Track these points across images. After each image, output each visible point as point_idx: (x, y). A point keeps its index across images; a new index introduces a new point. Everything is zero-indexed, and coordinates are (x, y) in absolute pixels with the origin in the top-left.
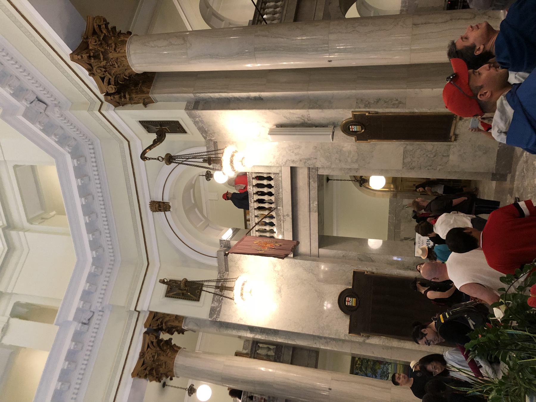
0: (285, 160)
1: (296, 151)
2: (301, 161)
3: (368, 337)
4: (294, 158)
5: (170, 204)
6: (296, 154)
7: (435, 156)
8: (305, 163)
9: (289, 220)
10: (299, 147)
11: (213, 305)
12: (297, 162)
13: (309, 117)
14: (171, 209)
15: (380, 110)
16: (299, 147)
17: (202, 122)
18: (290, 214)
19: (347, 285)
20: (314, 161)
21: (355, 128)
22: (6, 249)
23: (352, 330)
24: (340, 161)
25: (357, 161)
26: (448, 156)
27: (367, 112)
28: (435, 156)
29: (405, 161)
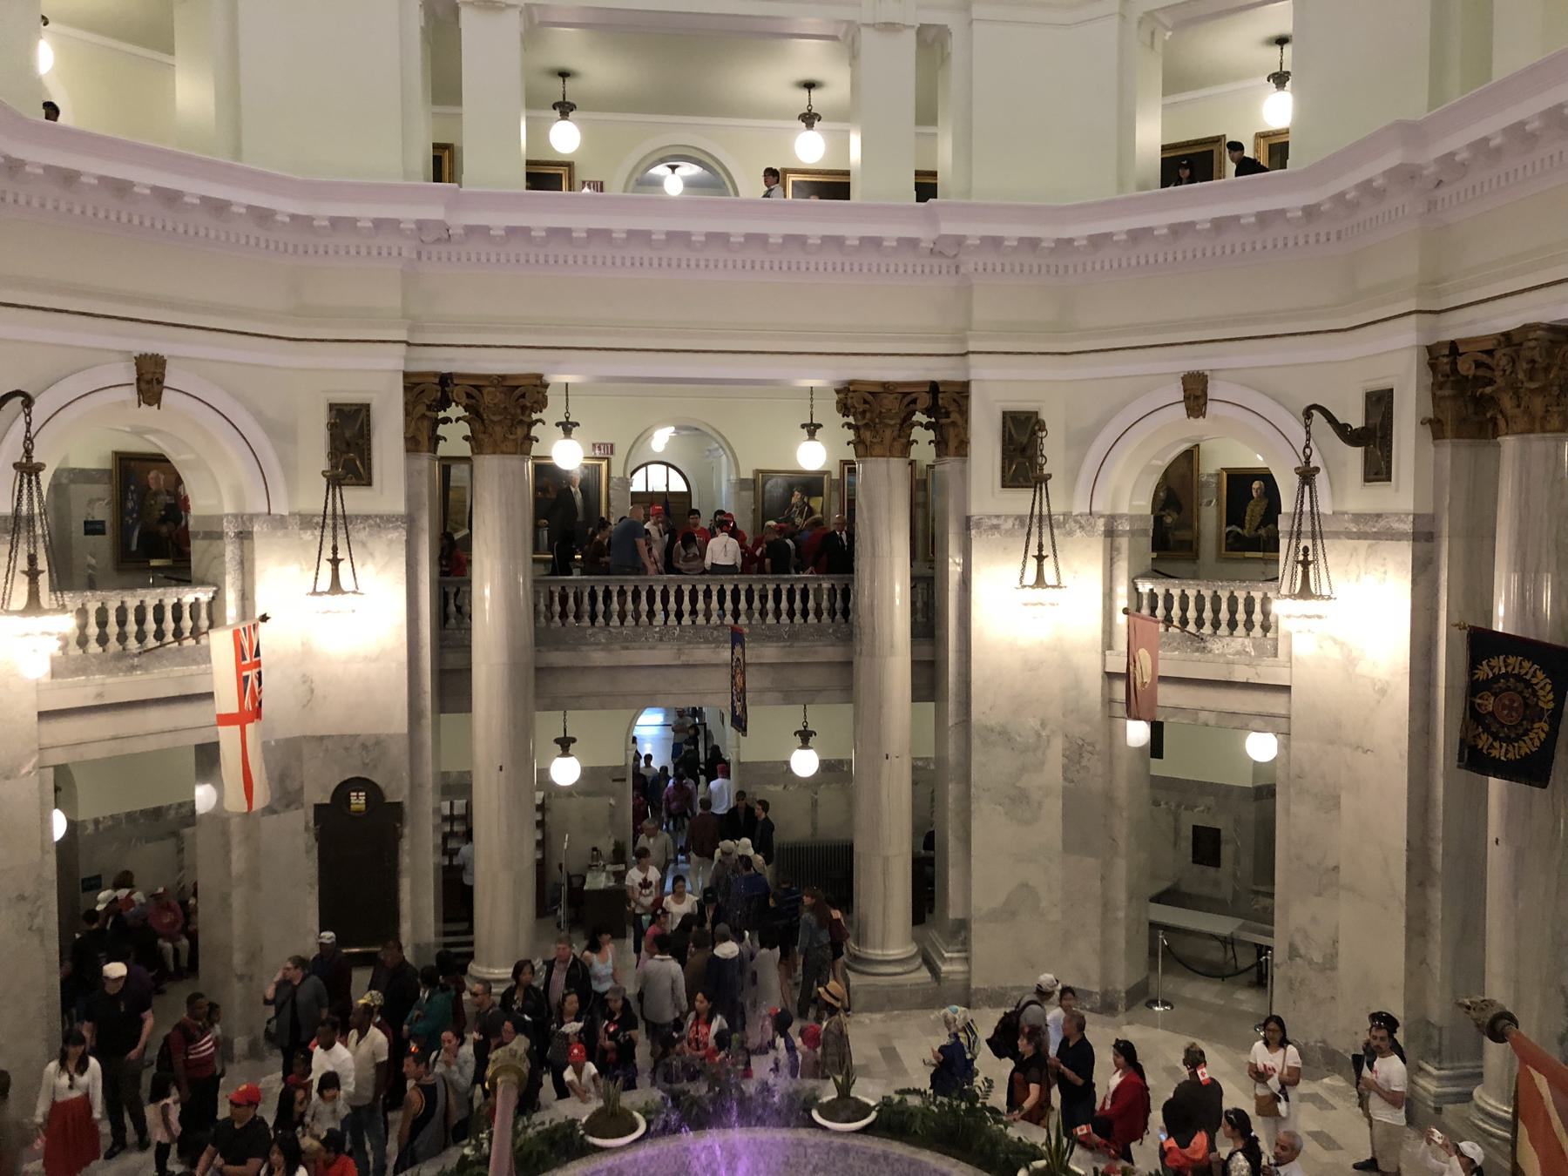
15: (405, 845)
21: (358, 801)
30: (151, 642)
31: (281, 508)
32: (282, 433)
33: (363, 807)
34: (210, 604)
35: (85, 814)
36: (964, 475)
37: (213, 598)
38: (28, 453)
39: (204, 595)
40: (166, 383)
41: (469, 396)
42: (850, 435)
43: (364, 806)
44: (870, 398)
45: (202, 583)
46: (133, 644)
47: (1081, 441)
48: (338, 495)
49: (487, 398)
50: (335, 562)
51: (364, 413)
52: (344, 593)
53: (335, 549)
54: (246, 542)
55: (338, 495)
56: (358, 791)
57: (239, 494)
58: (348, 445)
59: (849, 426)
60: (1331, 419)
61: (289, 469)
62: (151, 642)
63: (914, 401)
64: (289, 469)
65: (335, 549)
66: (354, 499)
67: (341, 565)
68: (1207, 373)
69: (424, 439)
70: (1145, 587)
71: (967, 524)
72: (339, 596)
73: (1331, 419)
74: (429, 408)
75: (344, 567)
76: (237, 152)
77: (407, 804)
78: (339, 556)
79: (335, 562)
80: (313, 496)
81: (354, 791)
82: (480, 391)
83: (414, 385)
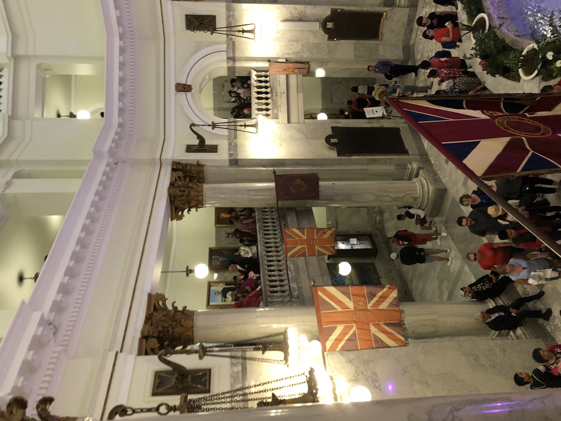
0: (283, 53)
1: (290, 48)
2: (293, 53)
3: (351, 156)
4: (289, 51)
5: (192, 86)
6: (290, 49)
7: (371, 50)
8: (296, 55)
9: (285, 96)
10: (292, 45)
11: (230, 152)
12: (290, 54)
13: (305, 13)
14: (192, 91)
15: (346, 8)
16: (292, 45)
17: (233, 15)
18: (285, 91)
19: (330, 132)
20: (302, 53)
22: (6, 135)
23: (339, 155)
24: (318, 53)
25: (328, 54)
26: (378, 50)
27: (339, 9)
28: (371, 50)
29: (356, 53)
30: (269, 90)
31: (224, 47)
32: (198, 47)
33: (332, 23)
34: (257, 71)
35: (320, 106)
37: (255, 70)
38: (209, 125)
39: (254, 73)
40: (184, 83)
42: (193, 210)
43: (332, 23)
45: (250, 73)
46: (269, 96)
48: (219, 29)
50: (243, 31)
51: (189, 17)
52: (254, 29)
53: (239, 31)
54: (236, 59)
55: (219, 29)
56: (326, 25)
58: (201, 24)
59: (189, 211)
62: (269, 90)
65: (239, 31)
66: (221, 23)
67: (245, 29)
72: (256, 31)
75: (245, 28)
76: (102, 59)
77: (331, 7)
78: (242, 30)
79: (243, 31)
80: (220, 38)
81: (326, 26)
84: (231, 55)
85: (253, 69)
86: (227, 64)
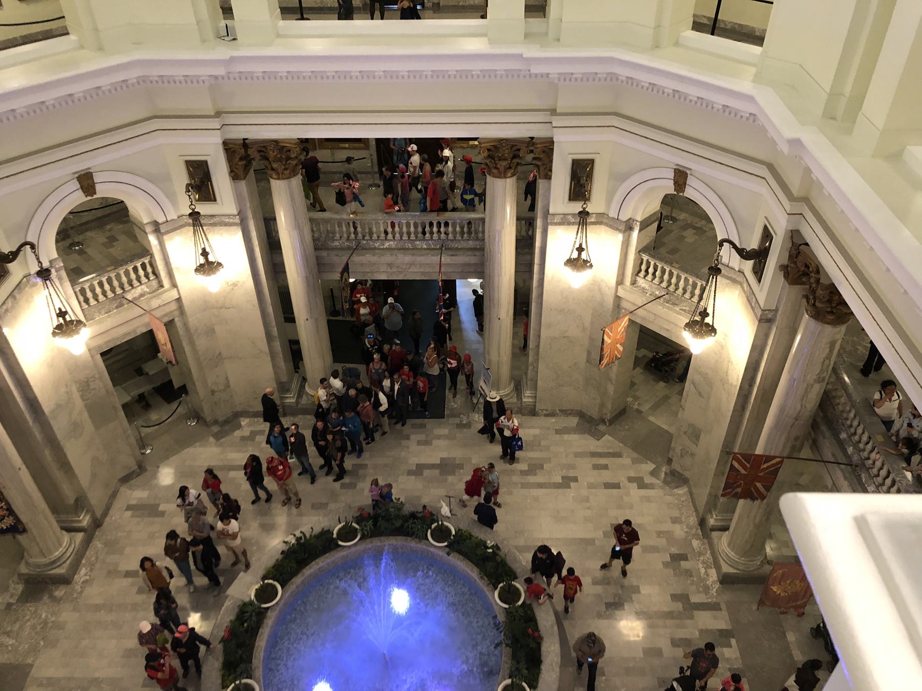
31: (172, 215)
36: (549, 189)
41: (259, 151)
44: (492, 148)
47: (619, 178)
49: (271, 153)
57: (148, 212)
60: (735, 246)
61: (172, 197)
63: (519, 150)
64: (172, 197)
68: (688, 172)
69: (240, 172)
70: (645, 257)
71: (546, 213)
73: (735, 246)
74: (241, 159)
82: (266, 148)
83: (230, 148)
84: (163, 229)
85: (151, 257)
86: (147, 224)
